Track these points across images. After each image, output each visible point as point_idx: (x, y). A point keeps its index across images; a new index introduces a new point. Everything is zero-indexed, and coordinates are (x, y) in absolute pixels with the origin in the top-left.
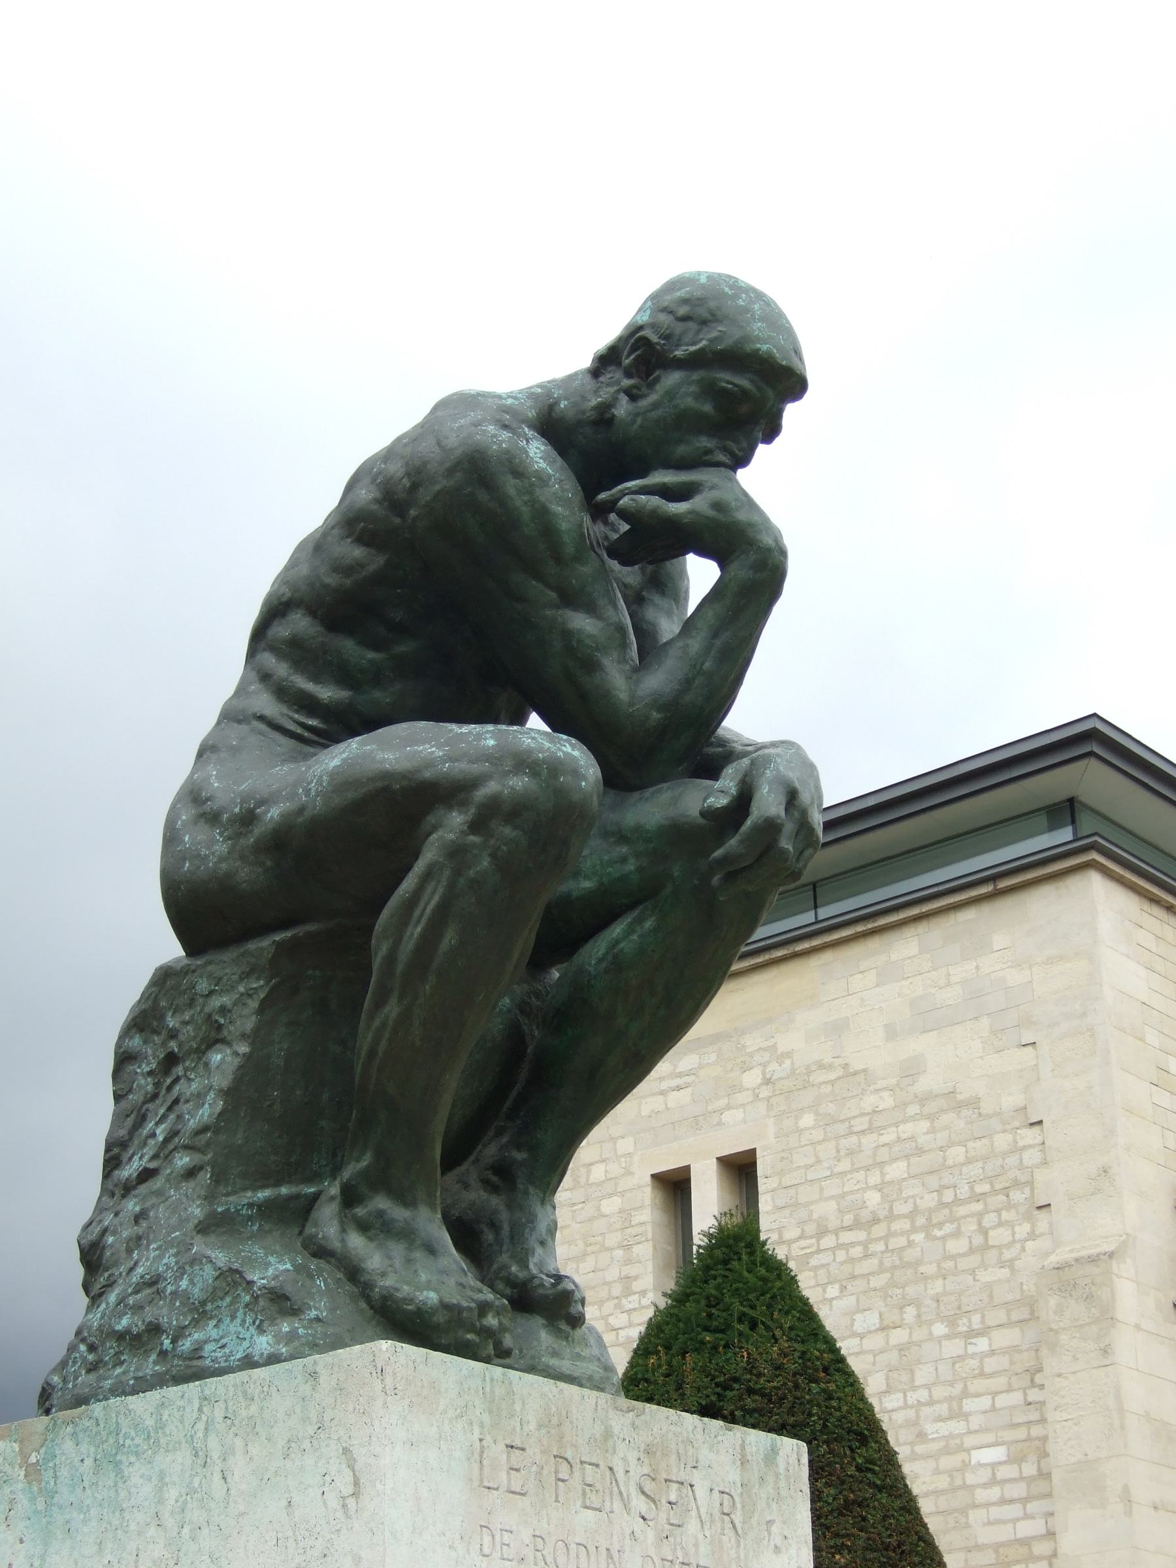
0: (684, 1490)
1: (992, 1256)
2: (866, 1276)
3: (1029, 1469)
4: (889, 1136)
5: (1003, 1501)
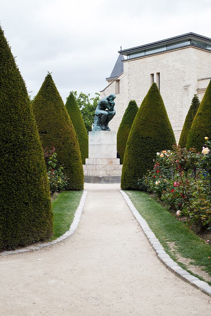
1: (180, 85)
2: (169, 86)
3: (182, 105)
4: (172, 72)
5: (180, 107)
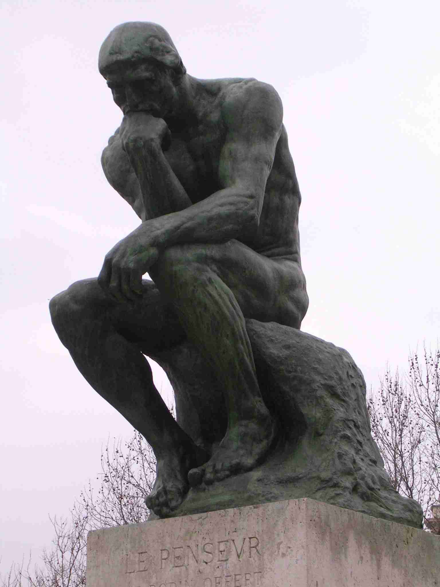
0: (228, 544)
